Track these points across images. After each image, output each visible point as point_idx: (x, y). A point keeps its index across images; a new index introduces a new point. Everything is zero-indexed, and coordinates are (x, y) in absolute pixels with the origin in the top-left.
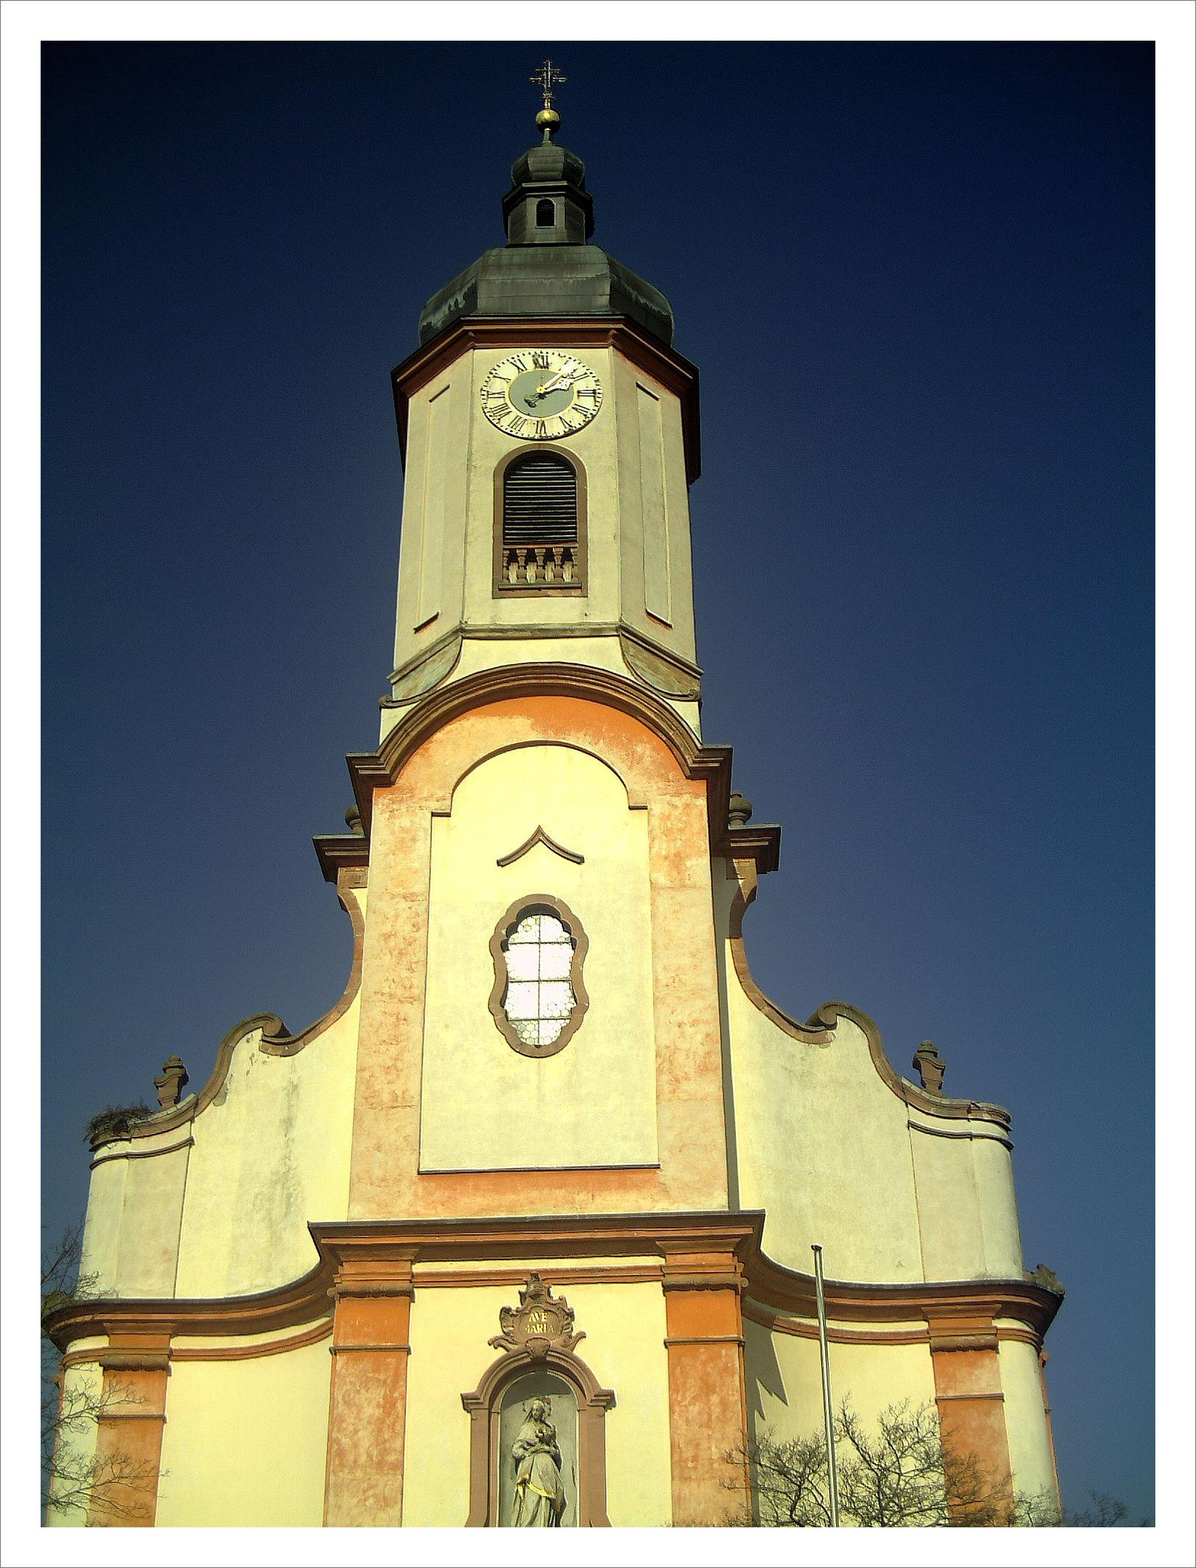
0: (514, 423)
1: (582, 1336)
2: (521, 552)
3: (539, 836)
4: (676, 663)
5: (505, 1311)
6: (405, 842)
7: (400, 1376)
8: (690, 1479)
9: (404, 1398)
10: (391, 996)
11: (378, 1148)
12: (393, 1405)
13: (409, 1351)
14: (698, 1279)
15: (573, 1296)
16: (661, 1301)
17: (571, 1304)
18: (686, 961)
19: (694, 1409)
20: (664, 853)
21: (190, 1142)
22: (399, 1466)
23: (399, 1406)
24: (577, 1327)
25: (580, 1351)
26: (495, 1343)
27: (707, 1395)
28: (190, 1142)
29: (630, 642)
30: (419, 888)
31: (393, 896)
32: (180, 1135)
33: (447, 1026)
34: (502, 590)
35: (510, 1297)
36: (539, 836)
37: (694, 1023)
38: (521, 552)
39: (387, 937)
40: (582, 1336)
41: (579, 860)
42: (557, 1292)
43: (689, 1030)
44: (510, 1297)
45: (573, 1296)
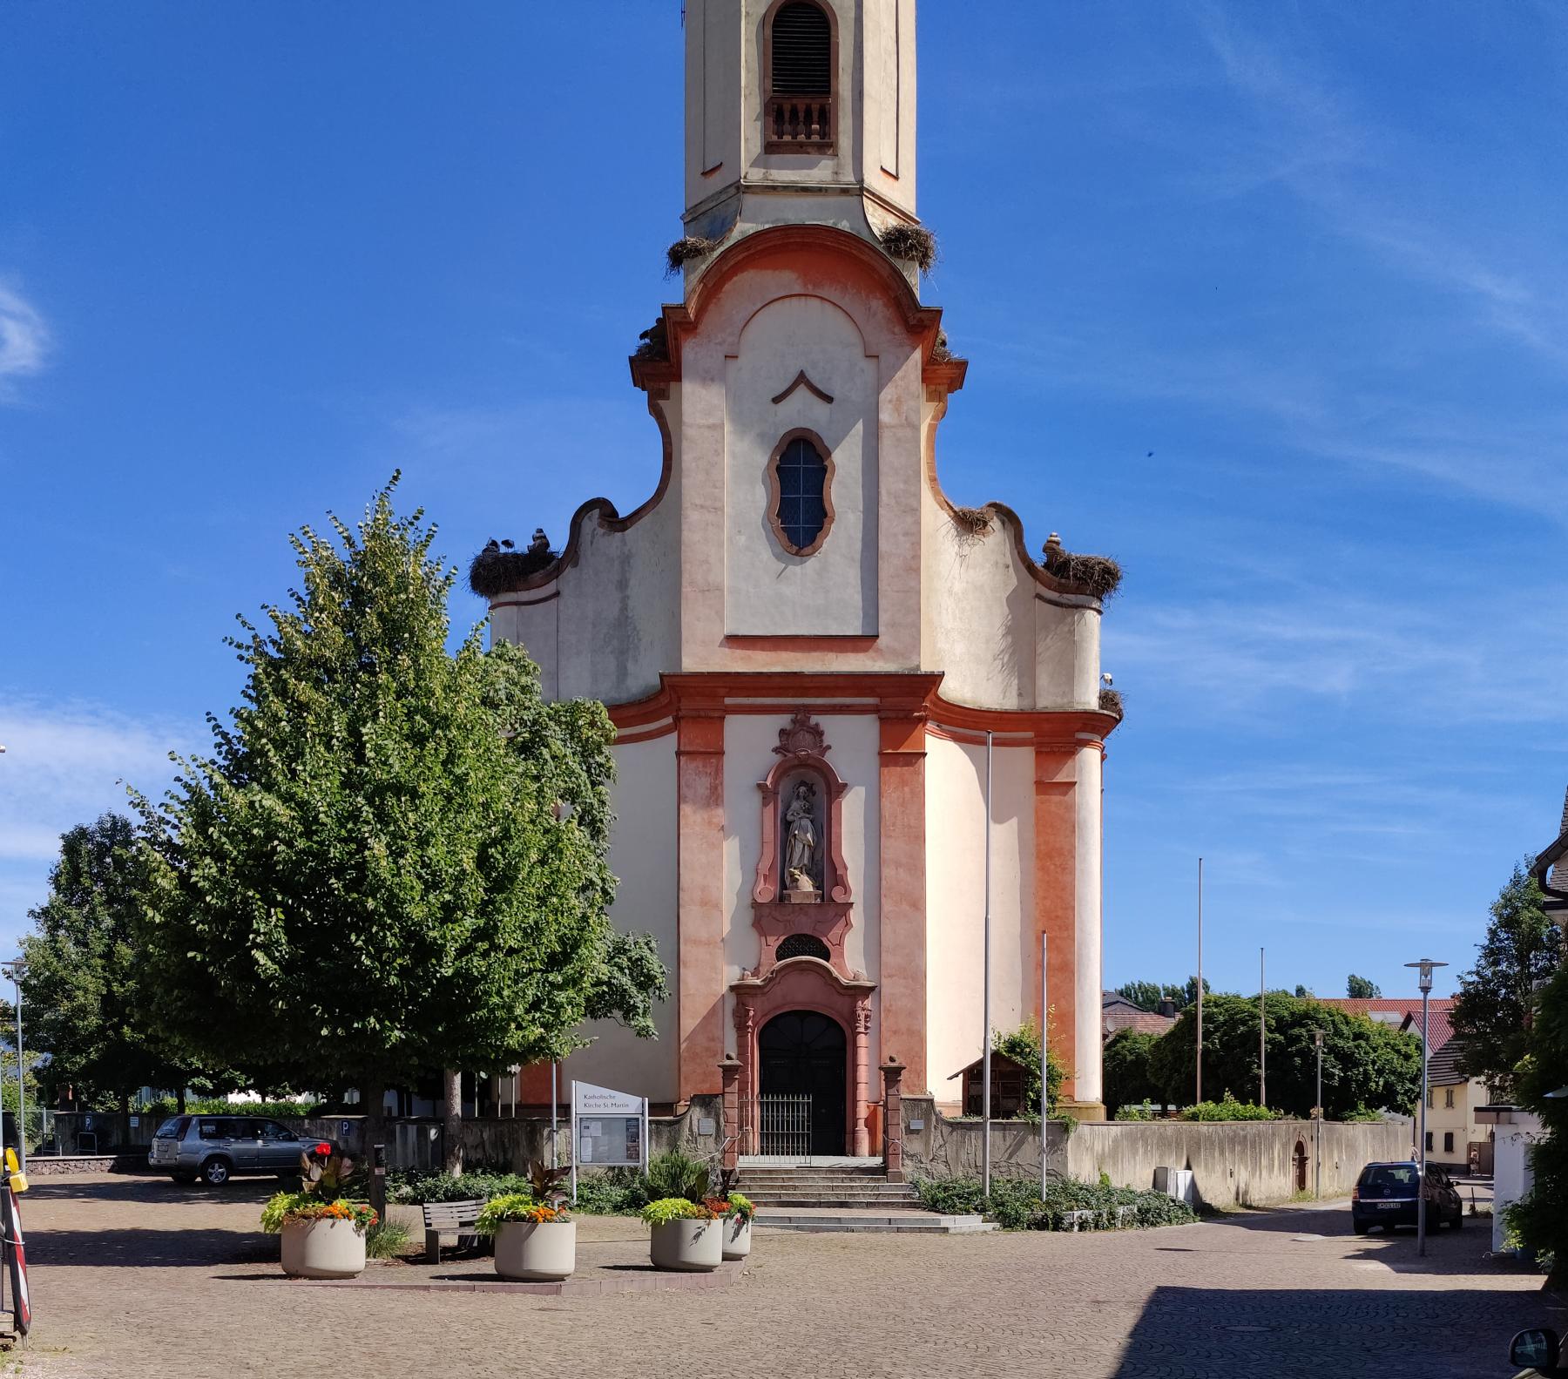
1: (829, 747)
2: (787, 107)
3: (802, 379)
5: (782, 732)
7: (718, 771)
8: (891, 836)
9: (722, 784)
10: (702, 507)
11: (698, 620)
12: (716, 788)
13: (722, 753)
14: (901, 715)
15: (826, 722)
16: (878, 724)
17: (823, 727)
18: (902, 486)
20: (889, 397)
23: (719, 788)
24: (827, 741)
25: (829, 758)
26: (776, 750)
27: (903, 787)
29: (869, 202)
31: (700, 427)
33: (739, 532)
35: (784, 721)
36: (802, 379)
37: (906, 534)
38: (787, 107)
40: (829, 747)
41: (828, 399)
42: (814, 719)
43: (901, 538)
44: (784, 721)
45: (826, 722)
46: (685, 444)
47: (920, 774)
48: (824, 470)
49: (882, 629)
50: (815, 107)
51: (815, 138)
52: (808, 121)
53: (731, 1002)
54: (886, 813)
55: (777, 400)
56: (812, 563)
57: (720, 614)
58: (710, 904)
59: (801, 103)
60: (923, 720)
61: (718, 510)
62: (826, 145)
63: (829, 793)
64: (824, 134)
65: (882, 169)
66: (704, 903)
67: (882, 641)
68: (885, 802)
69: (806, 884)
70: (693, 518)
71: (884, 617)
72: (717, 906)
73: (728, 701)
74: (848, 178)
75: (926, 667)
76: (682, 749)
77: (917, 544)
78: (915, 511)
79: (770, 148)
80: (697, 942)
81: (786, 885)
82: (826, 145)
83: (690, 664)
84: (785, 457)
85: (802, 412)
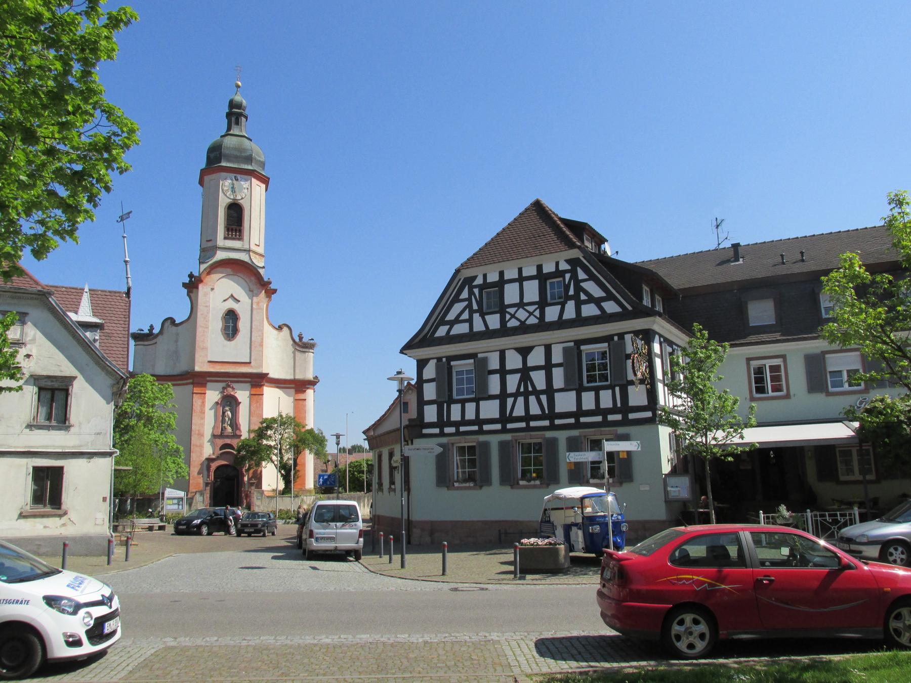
0: (230, 195)
4: (261, 255)
6: (206, 294)
7: (204, 398)
19: (255, 405)
21: (156, 343)
22: (204, 413)
28: (156, 343)
30: (208, 305)
32: (154, 341)
34: (225, 238)
35: (224, 385)
36: (232, 296)
38: (230, 229)
39: (202, 314)
44: (224, 385)
46: (199, 310)
47: (262, 399)
48: (237, 319)
49: (252, 361)
50: (238, 229)
51: (238, 236)
52: (236, 231)
53: (206, 463)
54: (252, 410)
55: (225, 301)
56: (233, 343)
57: (207, 356)
58: (201, 435)
59: (234, 227)
60: (264, 385)
61: (208, 328)
62: (240, 238)
63: (236, 404)
64: (240, 236)
65: (256, 245)
66: (199, 434)
67: (253, 364)
68: (252, 407)
69: (229, 429)
70: (199, 330)
71: (253, 358)
72: (203, 435)
73: (208, 379)
74: (246, 247)
75: (265, 371)
76: (194, 392)
77: (262, 339)
78: (261, 331)
79: (225, 238)
80: (197, 446)
81: (223, 429)
82: (240, 238)
83: (198, 368)
84: (226, 315)
85: (231, 304)
